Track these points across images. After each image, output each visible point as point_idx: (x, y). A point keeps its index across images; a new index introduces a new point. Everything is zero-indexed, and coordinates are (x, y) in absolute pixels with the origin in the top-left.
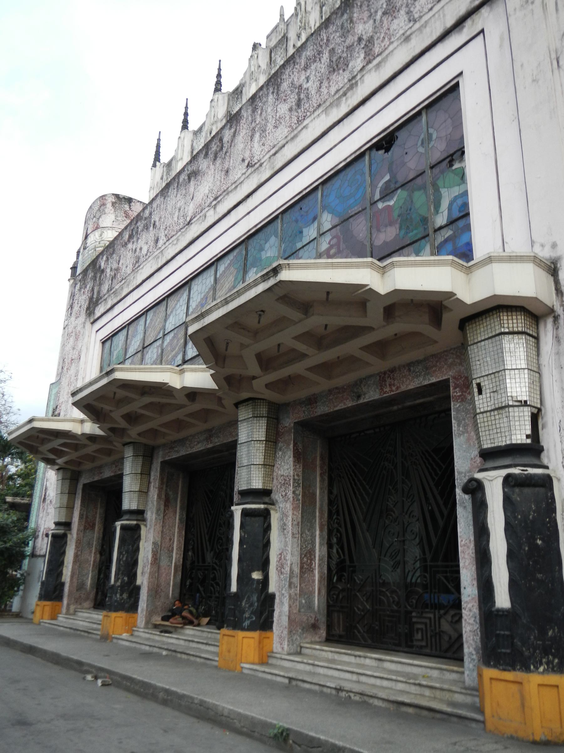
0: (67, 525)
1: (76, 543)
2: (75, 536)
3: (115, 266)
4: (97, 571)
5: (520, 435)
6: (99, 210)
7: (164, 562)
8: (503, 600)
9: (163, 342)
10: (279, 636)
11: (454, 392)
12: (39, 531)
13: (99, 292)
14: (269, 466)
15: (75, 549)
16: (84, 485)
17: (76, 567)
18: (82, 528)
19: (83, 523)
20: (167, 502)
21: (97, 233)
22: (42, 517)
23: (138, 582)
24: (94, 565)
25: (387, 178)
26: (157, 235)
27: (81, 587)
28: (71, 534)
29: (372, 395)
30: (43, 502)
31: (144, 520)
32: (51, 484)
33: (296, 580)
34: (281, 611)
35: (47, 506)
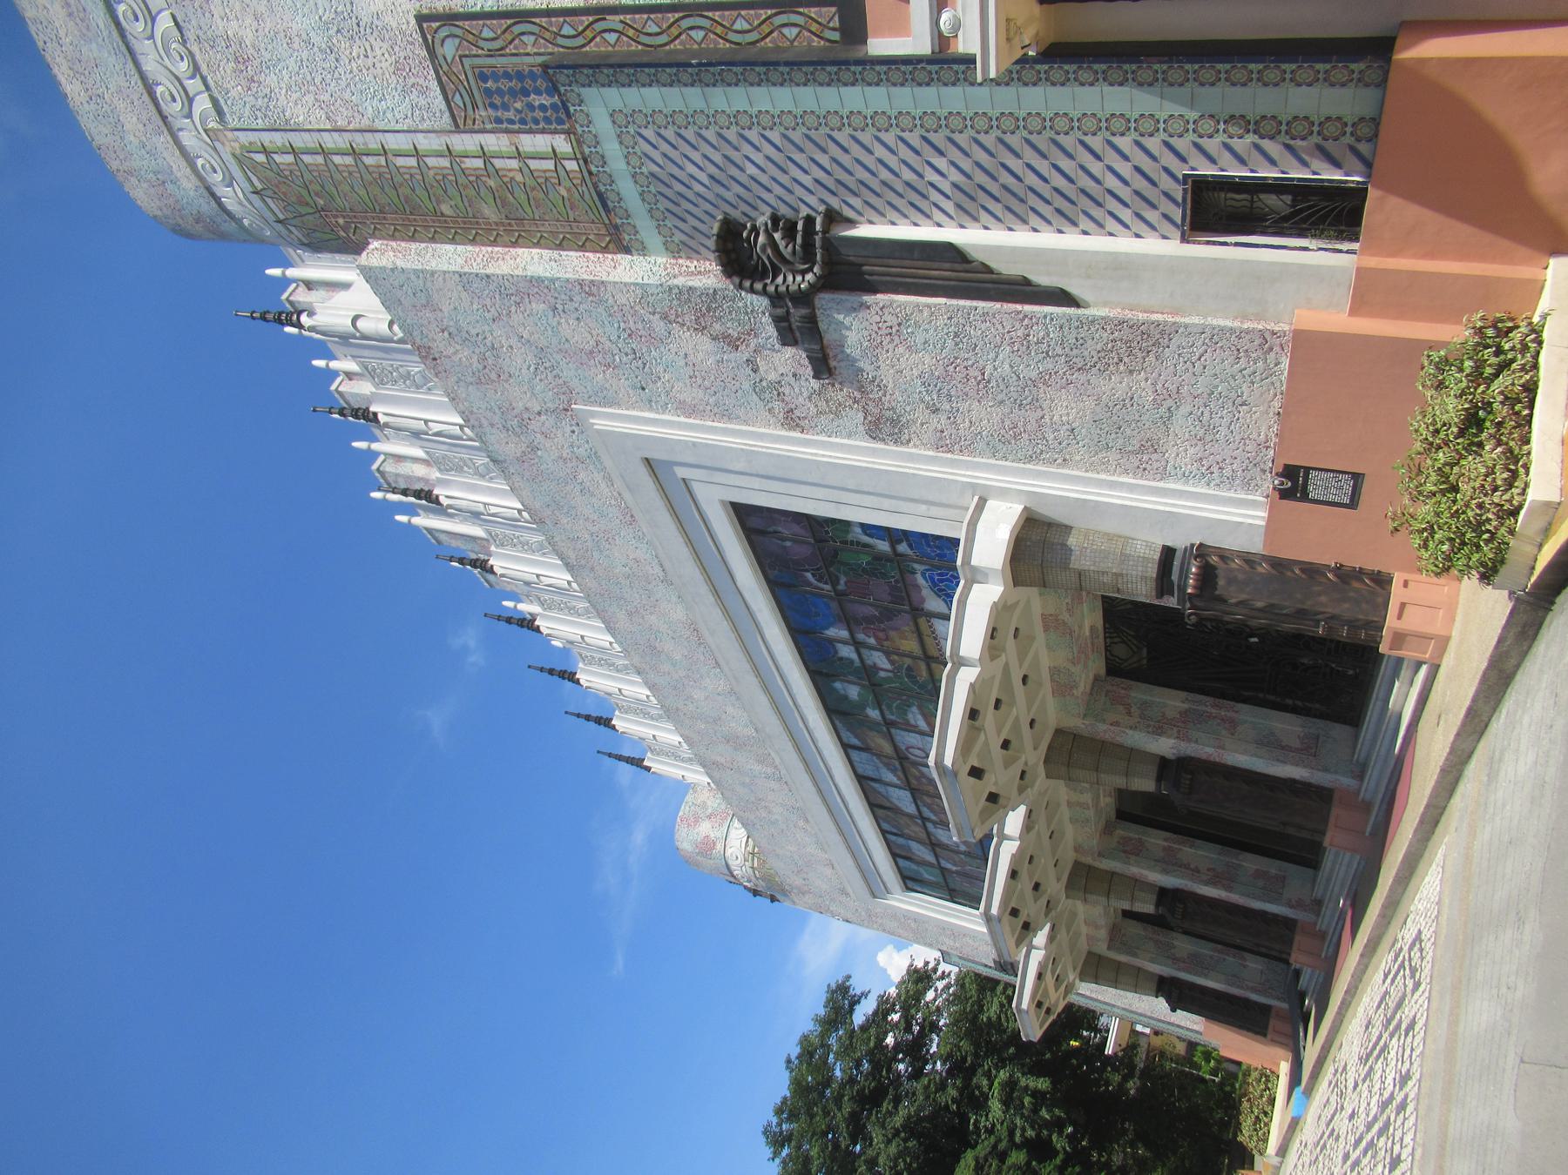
9: (928, 820)
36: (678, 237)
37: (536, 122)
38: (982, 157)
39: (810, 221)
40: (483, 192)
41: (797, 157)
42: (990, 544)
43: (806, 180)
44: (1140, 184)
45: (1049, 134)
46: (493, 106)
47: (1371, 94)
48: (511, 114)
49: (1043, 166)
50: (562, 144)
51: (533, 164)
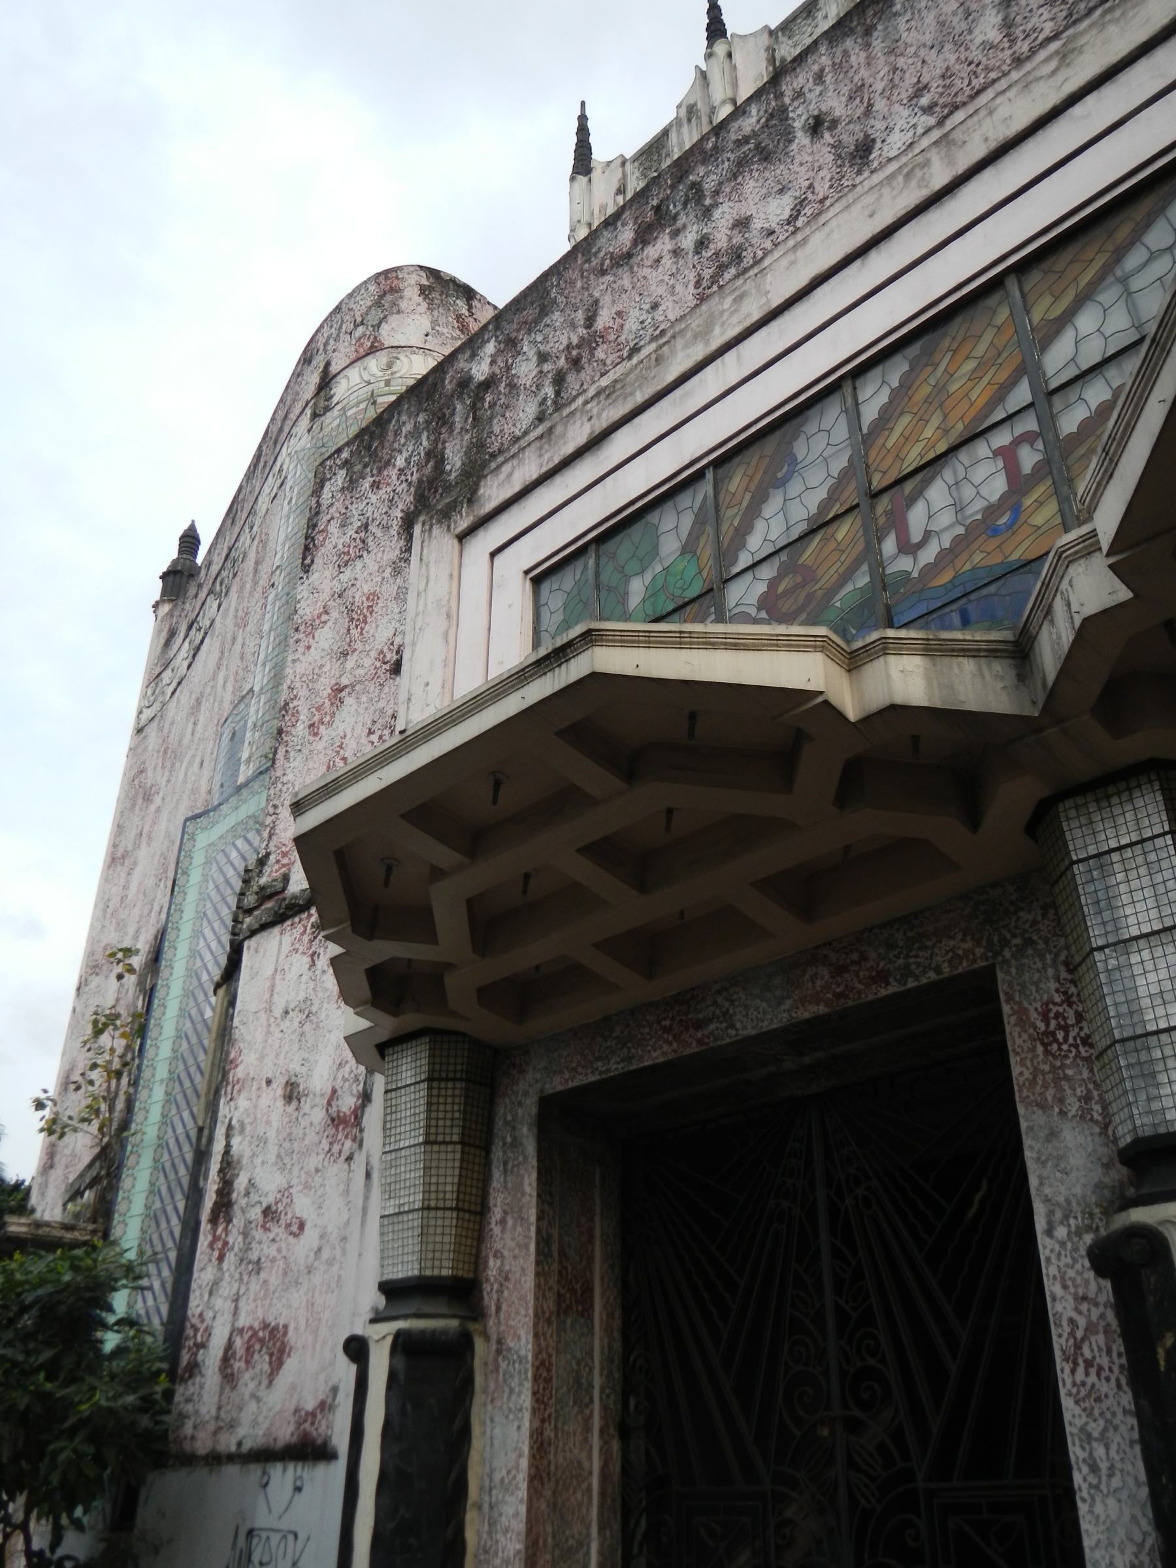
0: (461, 1291)
1: (536, 1378)
2: (523, 1343)
4: (616, 1527)
6: (378, 303)
12: (203, 1346)
15: (534, 1411)
16: (546, 1103)
17: (544, 1506)
18: (550, 1305)
19: (553, 1280)
21: (374, 364)
22: (216, 1284)
24: (603, 1494)
26: (849, 141)
28: (486, 1337)
30: (214, 1220)
32: (262, 1141)
35: (245, 1234)
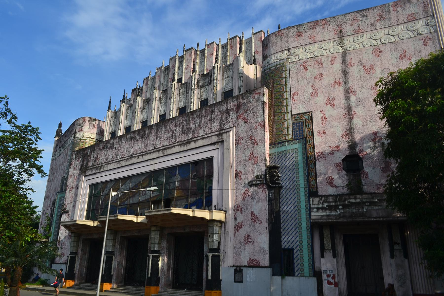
0: (76, 253)
3: (95, 156)
5: (216, 247)
7: (120, 268)
8: (210, 278)
10: (160, 289)
11: (205, 234)
13: (87, 164)
14: (159, 244)
20: (121, 249)
21: (81, 133)
23: (112, 274)
25: (195, 173)
27: (81, 275)
29: (188, 230)
31: (114, 254)
33: (166, 274)
34: (162, 281)
36: (274, 157)
37: (294, 132)
38: (294, 215)
39: (280, 183)
40: (280, 118)
41: (291, 183)
42: (218, 216)
43: (287, 184)
44: (291, 242)
45: (298, 226)
46: (296, 124)
47: (308, 275)
48: (295, 127)
49: (293, 225)
50: (291, 137)
51: (286, 130)
